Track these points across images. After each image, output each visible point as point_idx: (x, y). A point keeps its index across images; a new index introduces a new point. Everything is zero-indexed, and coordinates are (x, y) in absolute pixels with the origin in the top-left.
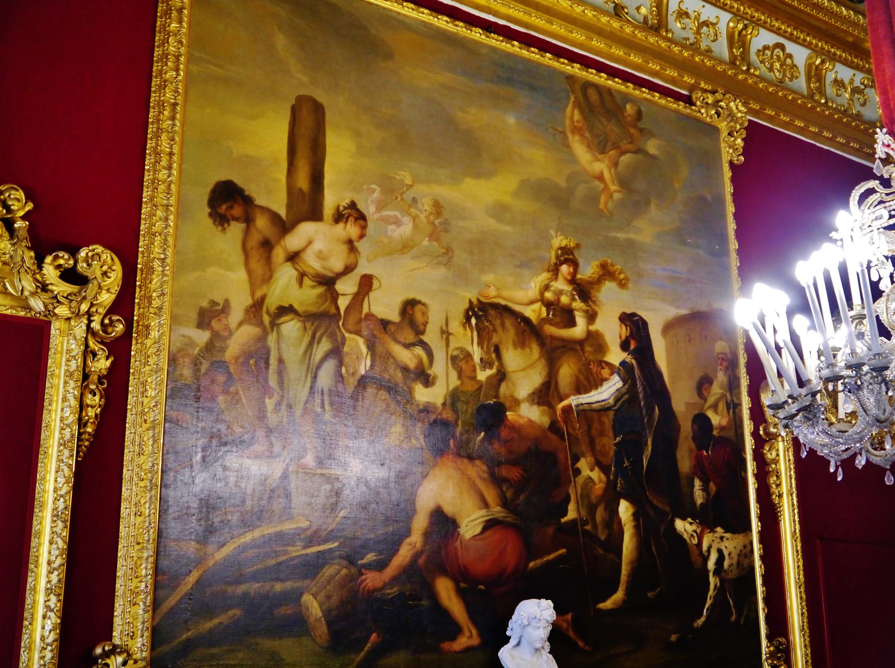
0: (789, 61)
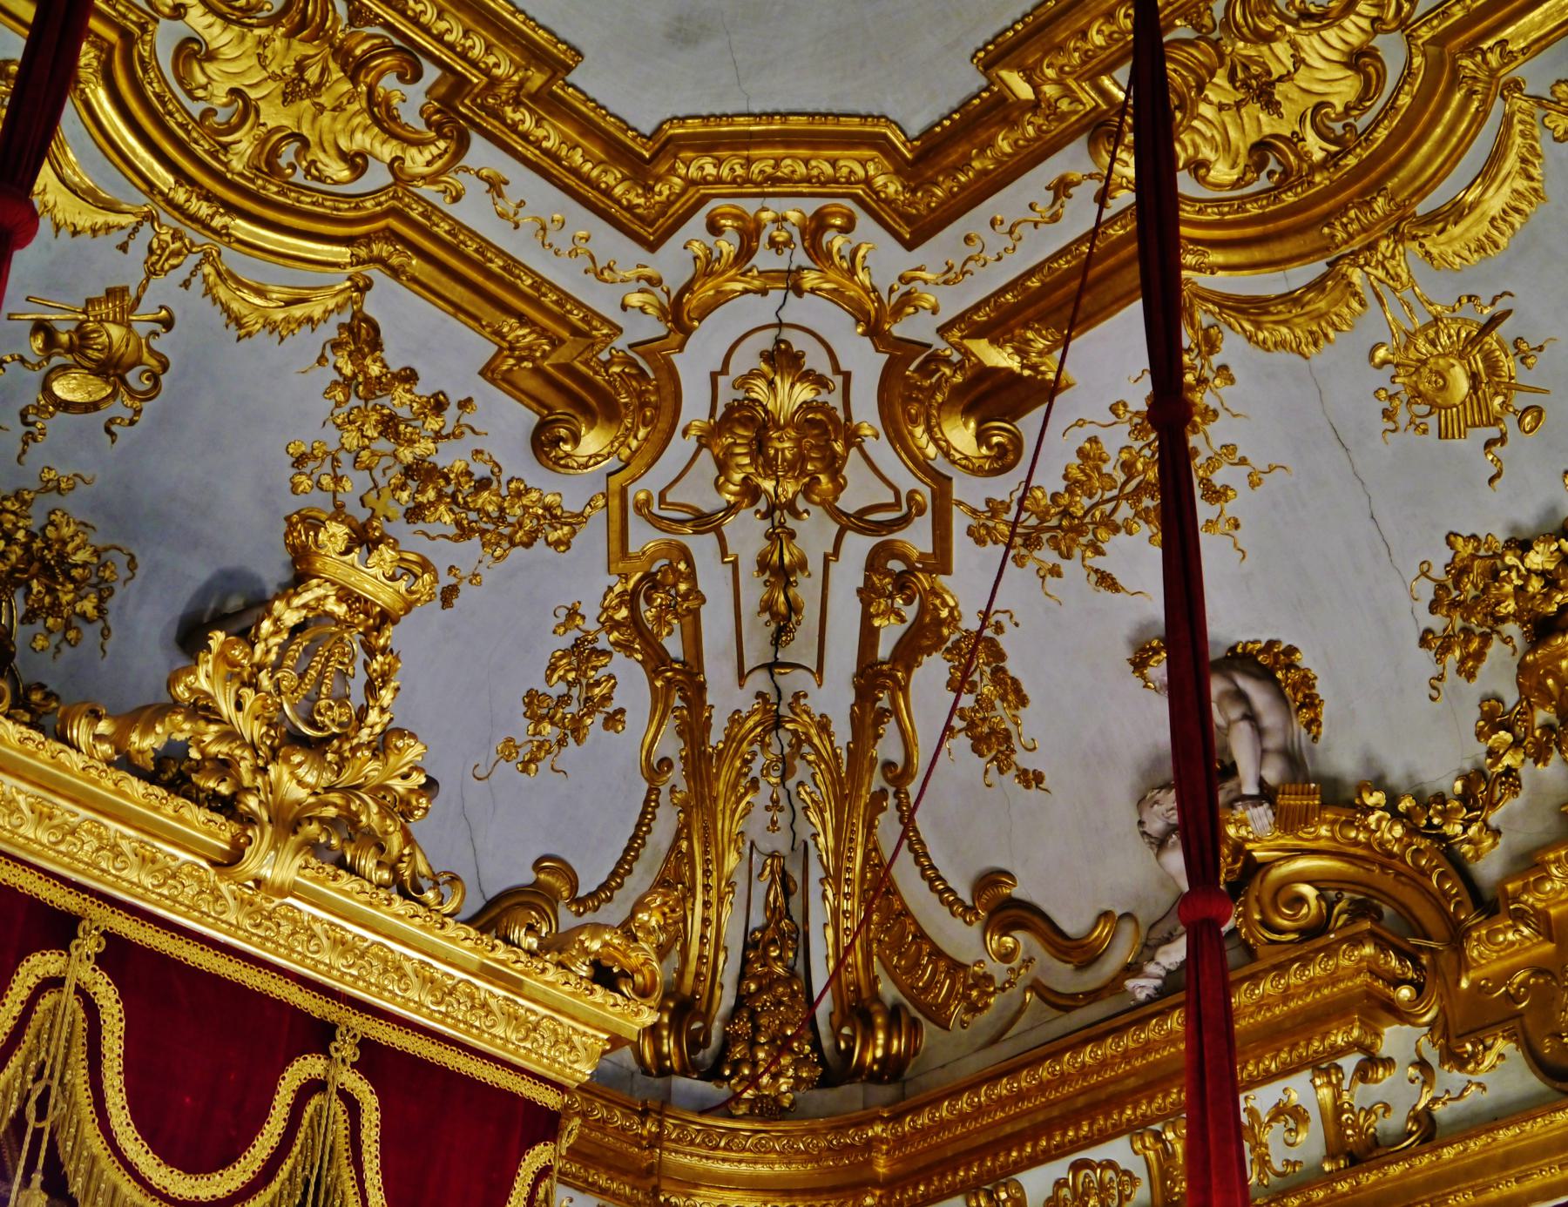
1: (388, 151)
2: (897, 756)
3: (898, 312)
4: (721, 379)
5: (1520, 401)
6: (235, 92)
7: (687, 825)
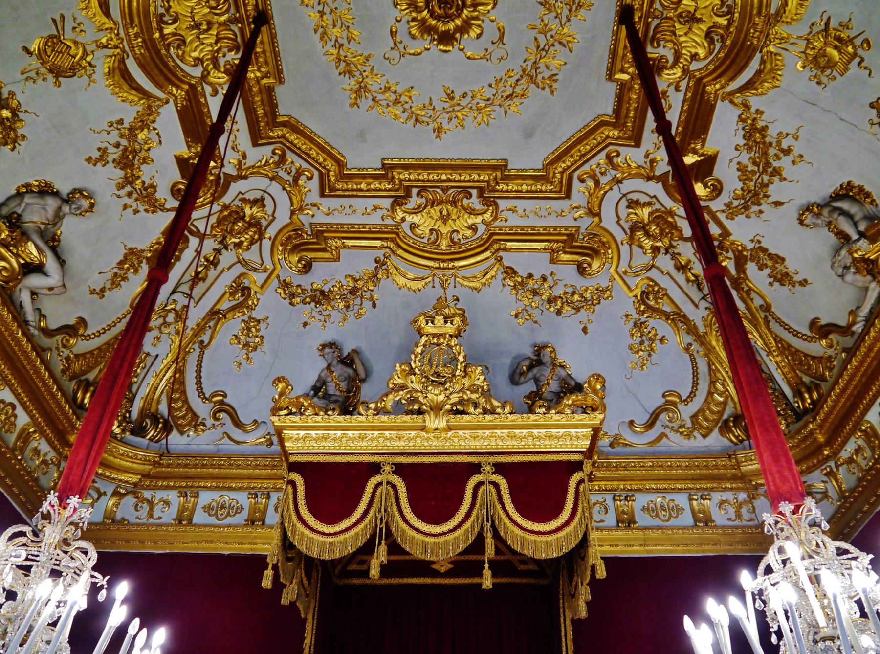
0: (12, 419)
1: (478, 219)
2: (761, 302)
3: (652, 168)
4: (622, 222)
5: (858, 42)
6: (431, 230)
7: (710, 360)
